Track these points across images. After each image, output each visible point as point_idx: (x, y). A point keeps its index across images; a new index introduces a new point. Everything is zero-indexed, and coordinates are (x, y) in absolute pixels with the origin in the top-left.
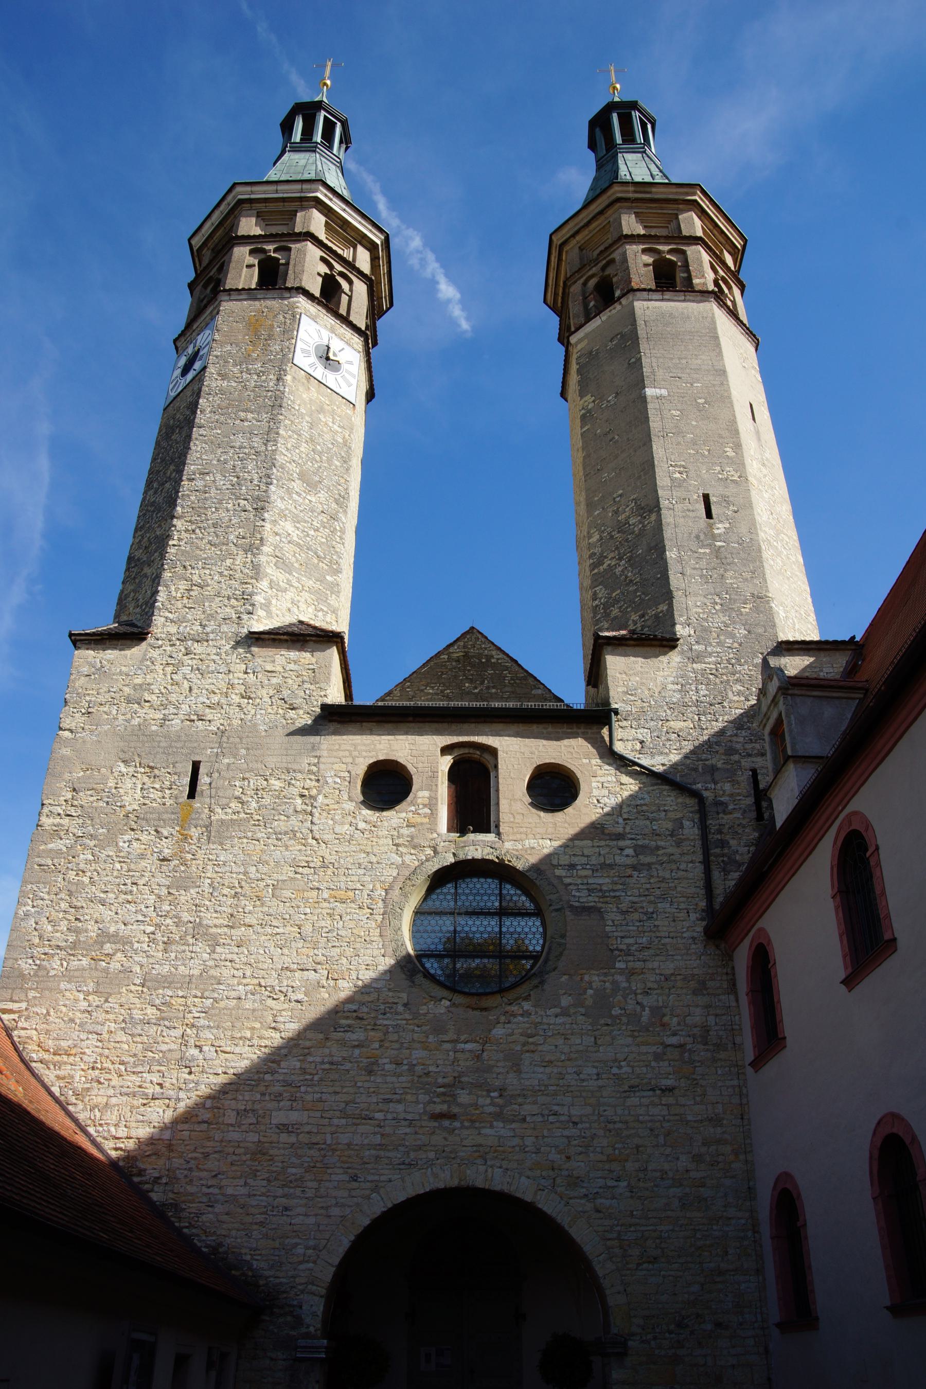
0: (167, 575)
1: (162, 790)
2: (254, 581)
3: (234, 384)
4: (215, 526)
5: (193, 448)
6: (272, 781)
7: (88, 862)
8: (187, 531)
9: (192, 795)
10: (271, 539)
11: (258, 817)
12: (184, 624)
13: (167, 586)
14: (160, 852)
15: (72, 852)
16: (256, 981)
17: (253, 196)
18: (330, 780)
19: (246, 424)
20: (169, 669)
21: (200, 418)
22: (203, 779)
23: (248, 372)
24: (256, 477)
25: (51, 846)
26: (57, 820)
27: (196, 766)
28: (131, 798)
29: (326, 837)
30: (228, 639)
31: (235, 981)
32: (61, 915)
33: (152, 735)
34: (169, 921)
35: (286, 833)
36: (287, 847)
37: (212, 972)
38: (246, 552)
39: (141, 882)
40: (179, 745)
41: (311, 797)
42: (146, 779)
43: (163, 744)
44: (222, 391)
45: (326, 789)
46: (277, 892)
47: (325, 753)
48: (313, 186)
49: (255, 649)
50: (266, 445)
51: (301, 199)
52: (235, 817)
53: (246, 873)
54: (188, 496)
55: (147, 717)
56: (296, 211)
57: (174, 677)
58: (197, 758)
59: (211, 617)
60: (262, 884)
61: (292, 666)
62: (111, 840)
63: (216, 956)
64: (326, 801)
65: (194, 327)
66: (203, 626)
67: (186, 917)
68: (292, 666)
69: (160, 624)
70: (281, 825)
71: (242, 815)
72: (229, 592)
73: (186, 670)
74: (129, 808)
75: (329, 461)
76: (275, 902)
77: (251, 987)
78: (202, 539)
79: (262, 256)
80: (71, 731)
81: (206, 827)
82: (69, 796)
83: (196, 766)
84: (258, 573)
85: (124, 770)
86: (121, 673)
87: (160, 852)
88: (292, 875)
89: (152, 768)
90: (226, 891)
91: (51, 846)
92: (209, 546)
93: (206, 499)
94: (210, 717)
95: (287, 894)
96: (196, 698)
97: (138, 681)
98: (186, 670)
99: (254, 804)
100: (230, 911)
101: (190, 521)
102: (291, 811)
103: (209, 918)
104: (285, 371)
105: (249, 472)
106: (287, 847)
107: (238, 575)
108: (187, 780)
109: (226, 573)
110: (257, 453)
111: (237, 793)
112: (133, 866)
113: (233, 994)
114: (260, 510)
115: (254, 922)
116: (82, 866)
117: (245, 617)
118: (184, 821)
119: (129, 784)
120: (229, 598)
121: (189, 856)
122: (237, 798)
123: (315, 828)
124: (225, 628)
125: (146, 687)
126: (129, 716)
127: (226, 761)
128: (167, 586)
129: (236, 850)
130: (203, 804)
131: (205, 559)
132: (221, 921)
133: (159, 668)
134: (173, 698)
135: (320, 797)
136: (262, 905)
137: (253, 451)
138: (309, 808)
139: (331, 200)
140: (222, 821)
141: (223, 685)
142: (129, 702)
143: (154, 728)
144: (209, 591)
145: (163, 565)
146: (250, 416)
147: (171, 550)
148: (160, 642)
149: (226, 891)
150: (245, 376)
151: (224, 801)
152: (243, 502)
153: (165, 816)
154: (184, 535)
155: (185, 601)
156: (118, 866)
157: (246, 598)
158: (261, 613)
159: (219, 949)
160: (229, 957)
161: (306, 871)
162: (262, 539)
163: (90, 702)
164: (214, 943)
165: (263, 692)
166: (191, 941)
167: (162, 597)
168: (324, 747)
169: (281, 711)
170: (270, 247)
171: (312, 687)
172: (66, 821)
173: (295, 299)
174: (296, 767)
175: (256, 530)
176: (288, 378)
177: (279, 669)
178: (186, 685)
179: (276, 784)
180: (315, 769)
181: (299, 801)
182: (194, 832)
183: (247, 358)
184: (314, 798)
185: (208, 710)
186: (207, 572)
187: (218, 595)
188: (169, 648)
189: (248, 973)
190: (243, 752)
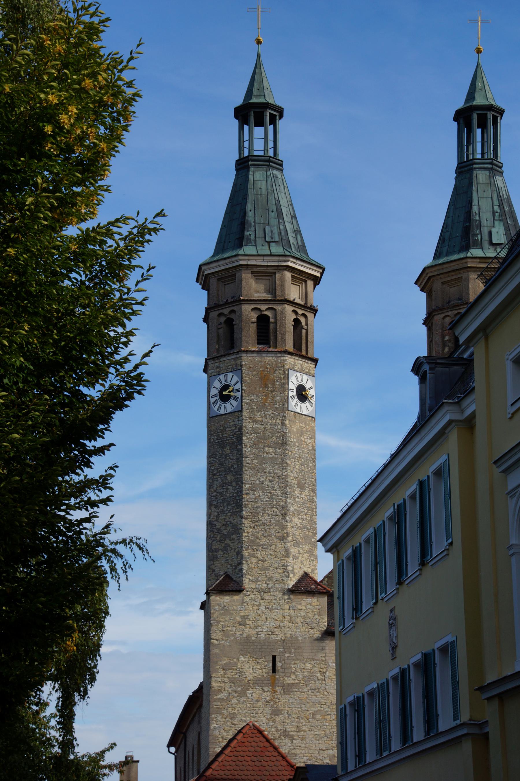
0: (246, 554)
1: (261, 669)
2: (286, 558)
3: (259, 426)
4: (264, 524)
5: (245, 472)
6: (307, 665)
7: (236, 704)
8: (250, 527)
9: (274, 670)
10: (291, 531)
11: (303, 682)
12: (258, 583)
13: (247, 561)
14: (265, 698)
15: (228, 699)
16: (310, 755)
17: (249, 263)
18: (331, 664)
19: (270, 456)
20: (255, 607)
21: (246, 450)
22: (278, 664)
23: (265, 417)
24: (279, 493)
25: (219, 696)
26: (219, 684)
27: (274, 658)
28: (249, 675)
29: (331, 691)
30: (280, 592)
31: (302, 755)
32: (229, 728)
33: (254, 642)
34: (273, 730)
35: (315, 690)
36: (316, 696)
37: (293, 751)
38: (281, 540)
39: (259, 712)
40: (266, 647)
41: (324, 672)
42: (253, 664)
43: (259, 647)
44: (254, 431)
45: (330, 669)
46: (314, 716)
47: (327, 651)
48: (287, 258)
49: (292, 597)
50: (281, 471)
51: (278, 266)
52: (293, 682)
53: (301, 708)
54: (248, 505)
55: (249, 633)
56: (275, 273)
57: (258, 612)
58: (274, 654)
59: (270, 579)
60: (308, 713)
61: (309, 607)
62: (243, 694)
63: (293, 744)
64: (330, 674)
65: (222, 360)
66: (267, 584)
67: (279, 727)
68: (309, 607)
69: (247, 583)
70: (312, 685)
71: (297, 681)
72: (276, 565)
73: (262, 608)
74: (249, 678)
75: (308, 465)
76: (314, 721)
77: (308, 758)
78: (259, 532)
79: (259, 313)
80: (217, 640)
81: (283, 687)
82: (222, 672)
83: (274, 658)
84: (288, 554)
85: (243, 660)
86: (234, 610)
87: (265, 698)
88: (319, 708)
89: (256, 658)
90: (294, 716)
91: (219, 696)
92: (263, 537)
93: (257, 507)
94: (277, 633)
95: (319, 717)
96: (270, 623)
97: (242, 614)
98: (262, 608)
99: (301, 676)
100: (296, 724)
101: (251, 521)
102: (316, 679)
103: (289, 728)
104: (285, 417)
105: (276, 490)
106: (316, 696)
107: (279, 555)
108: (271, 665)
109: (273, 553)
110: (278, 477)
111: (293, 671)
112: (255, 705)
113: (302, 760)
114: (284, 515)
115: (307, 729)
116: (234, 705)
117: (285, 579)
118: (273, 683)
119: (247, 666)
120: (276, 568)
121: (277, 700)
122: (294, 673)
123: (327, 687)
124: (277, 586)
125: (245, 617)
126: (241, 632)
127: (286, 655)
128: (247, 561)
129: (296, 698)
130: (279, 676)
131: (262, 545)
132: (293, 729)
133: (250, 607)
134: (259, 623)
135: (327, 672)
136: (309, 722)
137: (275, 476)
138: (323, 678)
139: (295, 263)
140: (289, 684)
141: (280, 616)
142: (240, 625)
143: (253, 638)
144: (266, 564)
145: (242, 547)
146: (271, 450)
147: (245, 539)
148: (249, 593)
149: (294, 716)
150: (265, 420)
151: (289, 674)
152: (275, 510)
153: (265, 682)
154: (250, 530)
155: (256, 570)
156: (248, 705)
157: (285, 567)
158: (291, 575)
159: (294, 741)
160: (299, 744)
161: (325, 706)
162: (287, 534)
163: (222, 625)
164: (292, 739)
165: (298, 620)
166: (283, 738)
167: (245, 567)
168: (327, 648)
169: (307, 630)
170: (263, 307)
171: (319, 617)
172: (223, 685)
173: (285, 358)
174: (316, 658)
175: (284, 528)
176: (287, 422)
177: (304, 608)
178: (264, 617)
179: (309, 666)
180: (324, 659)
181: (319, 674)
182: (278, 689)
183: (263, 407)
184: (325, 673)
185: (275, 630)
186: (264, 553)
187: (271, 565)
188: (253, 596)
189: (307, 752)
190: (293, 650)
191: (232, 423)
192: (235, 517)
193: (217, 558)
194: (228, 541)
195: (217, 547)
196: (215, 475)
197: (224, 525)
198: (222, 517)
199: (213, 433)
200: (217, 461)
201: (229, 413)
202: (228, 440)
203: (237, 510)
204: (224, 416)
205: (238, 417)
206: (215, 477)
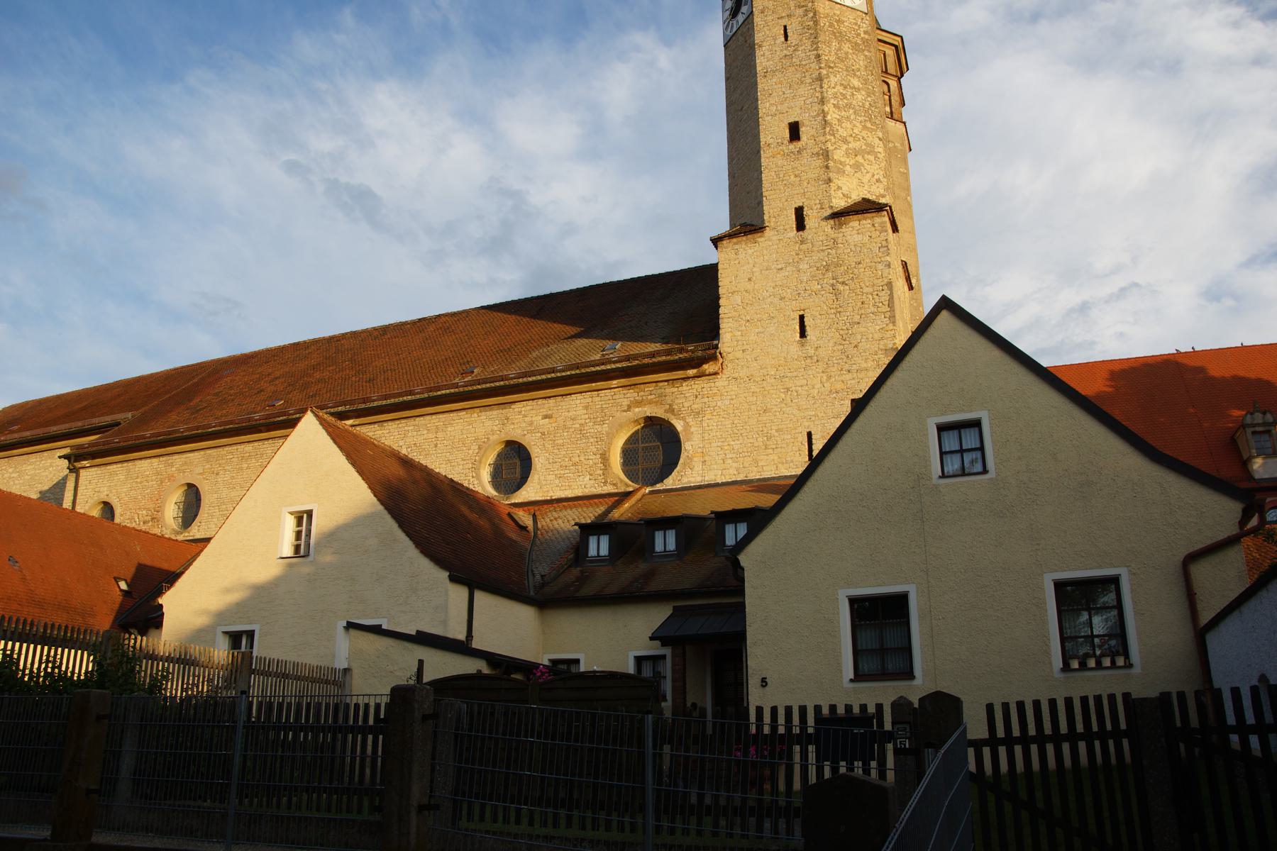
191: (854, 21)
192: (869, 134)
193: (844, 172)
194: (859, 158)
195: (843, 160)
196: (832, 68)
197: (851, 135)
198: (847, 125)
199: (822, 16)
200: (833, 53)
201: (848, 7)
202: (849, 37)
203: (872, 127)
204: (839, 6)
205: (862, 19)
206: (830, 70)
